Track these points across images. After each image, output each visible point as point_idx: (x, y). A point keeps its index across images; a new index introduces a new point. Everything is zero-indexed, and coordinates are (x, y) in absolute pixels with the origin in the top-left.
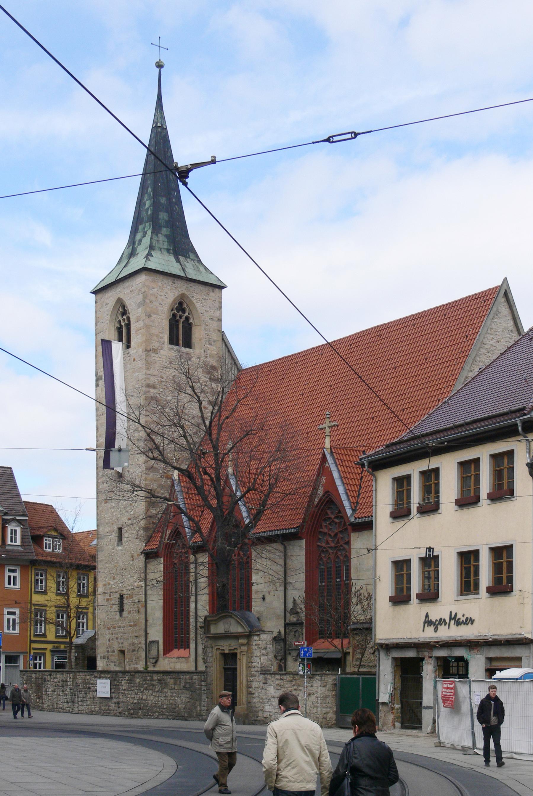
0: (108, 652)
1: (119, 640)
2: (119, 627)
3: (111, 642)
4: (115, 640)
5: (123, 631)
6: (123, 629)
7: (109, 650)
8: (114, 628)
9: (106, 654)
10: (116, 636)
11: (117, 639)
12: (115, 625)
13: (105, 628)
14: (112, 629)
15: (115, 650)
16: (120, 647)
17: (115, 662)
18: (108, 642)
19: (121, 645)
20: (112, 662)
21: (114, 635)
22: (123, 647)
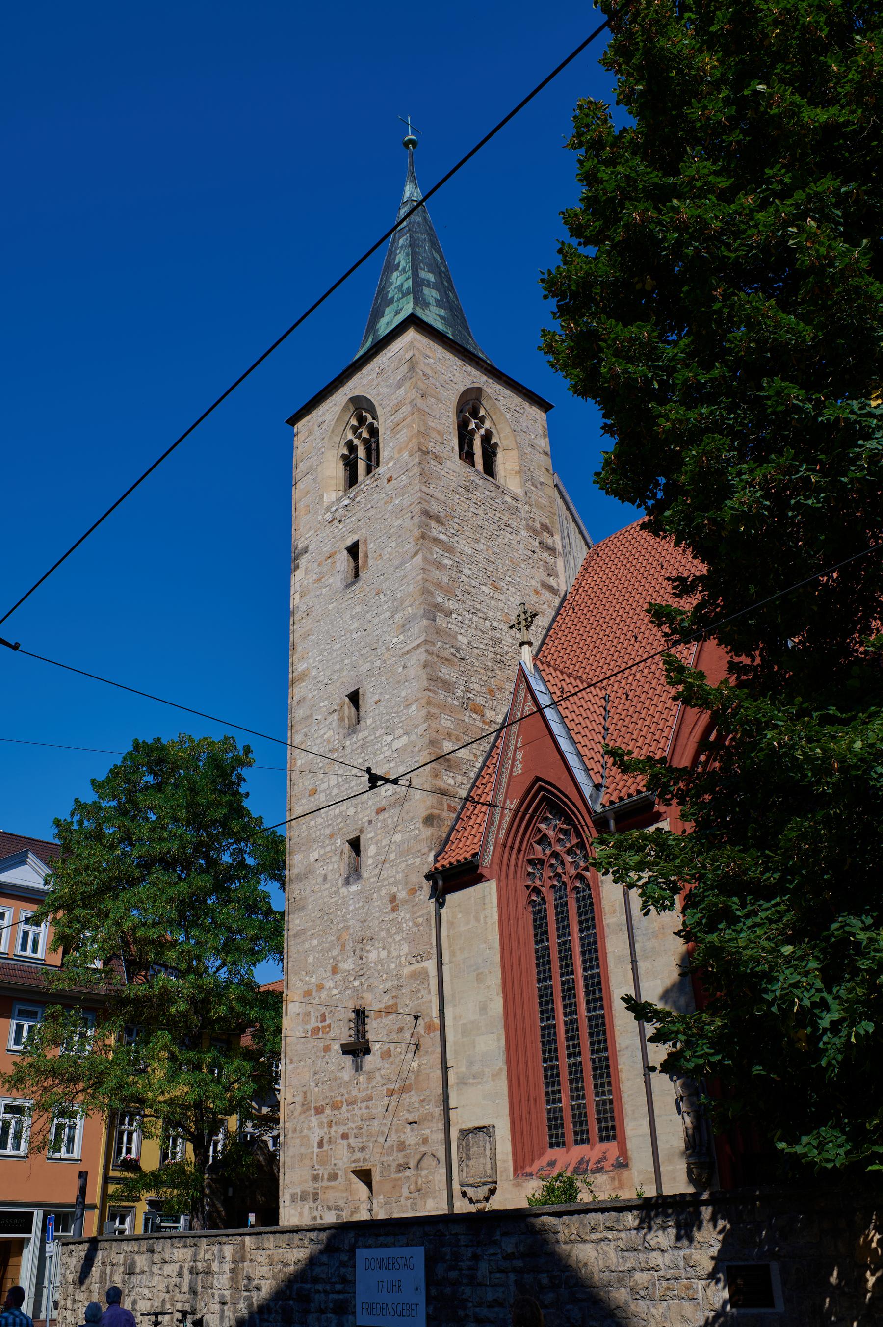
0: (315, 1178)
1: (351, 1140)
2: (352, 1103)
3: (326, 1147)
4: (339, 1140)
5: (364, 1111)
6: (364, 1105)
7: (320, 1172)
8: (336, 1107)
9: (310, 1186)
10: (342, 1129)
11: (345, 1136)
12: (339, 1099)
13: (309, 1109)
14: (328, 1111)
15: (340, 1173)
16: (354, 1161)
17: (337, 1208)
18: (316, 1150)
19: (358, 1155)
20: (329, 1208)
21: (334, 1128)
22: (364, 1160)
